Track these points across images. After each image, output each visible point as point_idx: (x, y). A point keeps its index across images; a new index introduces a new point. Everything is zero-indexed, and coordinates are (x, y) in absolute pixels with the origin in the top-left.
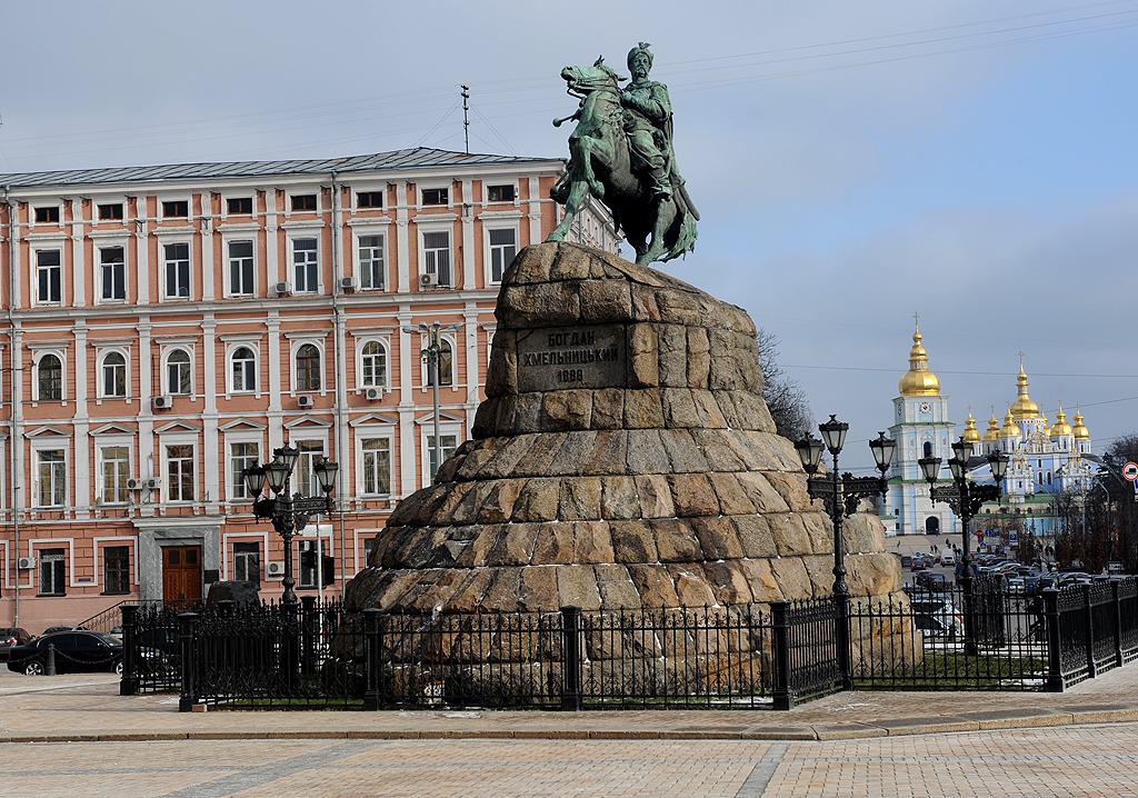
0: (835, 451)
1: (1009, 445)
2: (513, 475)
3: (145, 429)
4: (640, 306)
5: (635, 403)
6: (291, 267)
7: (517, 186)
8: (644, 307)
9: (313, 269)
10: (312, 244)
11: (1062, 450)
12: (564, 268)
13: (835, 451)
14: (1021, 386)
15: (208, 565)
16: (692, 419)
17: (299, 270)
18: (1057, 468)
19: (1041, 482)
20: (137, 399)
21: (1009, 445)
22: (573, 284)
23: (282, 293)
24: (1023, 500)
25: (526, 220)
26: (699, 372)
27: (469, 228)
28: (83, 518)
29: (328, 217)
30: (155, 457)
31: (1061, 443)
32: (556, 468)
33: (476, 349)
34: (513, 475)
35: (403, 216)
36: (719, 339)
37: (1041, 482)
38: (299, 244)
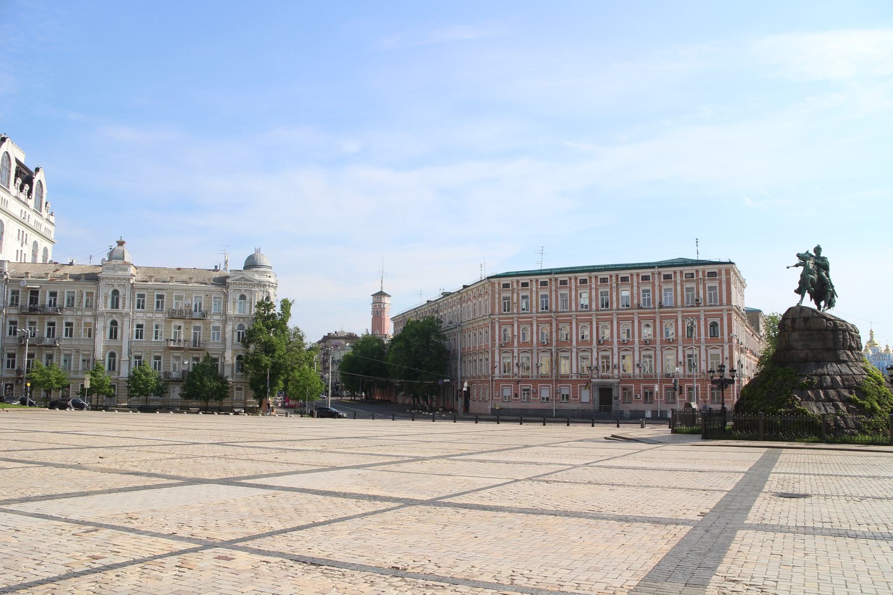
3: (595, 350)
9: (649, 299)
15: (614, 394)
17: (644, 300)
20: (591, 342)
23: (639, 307)
25: (720, 284)
27: (701, 286)
28: (575, 378)
30: (597, 359)
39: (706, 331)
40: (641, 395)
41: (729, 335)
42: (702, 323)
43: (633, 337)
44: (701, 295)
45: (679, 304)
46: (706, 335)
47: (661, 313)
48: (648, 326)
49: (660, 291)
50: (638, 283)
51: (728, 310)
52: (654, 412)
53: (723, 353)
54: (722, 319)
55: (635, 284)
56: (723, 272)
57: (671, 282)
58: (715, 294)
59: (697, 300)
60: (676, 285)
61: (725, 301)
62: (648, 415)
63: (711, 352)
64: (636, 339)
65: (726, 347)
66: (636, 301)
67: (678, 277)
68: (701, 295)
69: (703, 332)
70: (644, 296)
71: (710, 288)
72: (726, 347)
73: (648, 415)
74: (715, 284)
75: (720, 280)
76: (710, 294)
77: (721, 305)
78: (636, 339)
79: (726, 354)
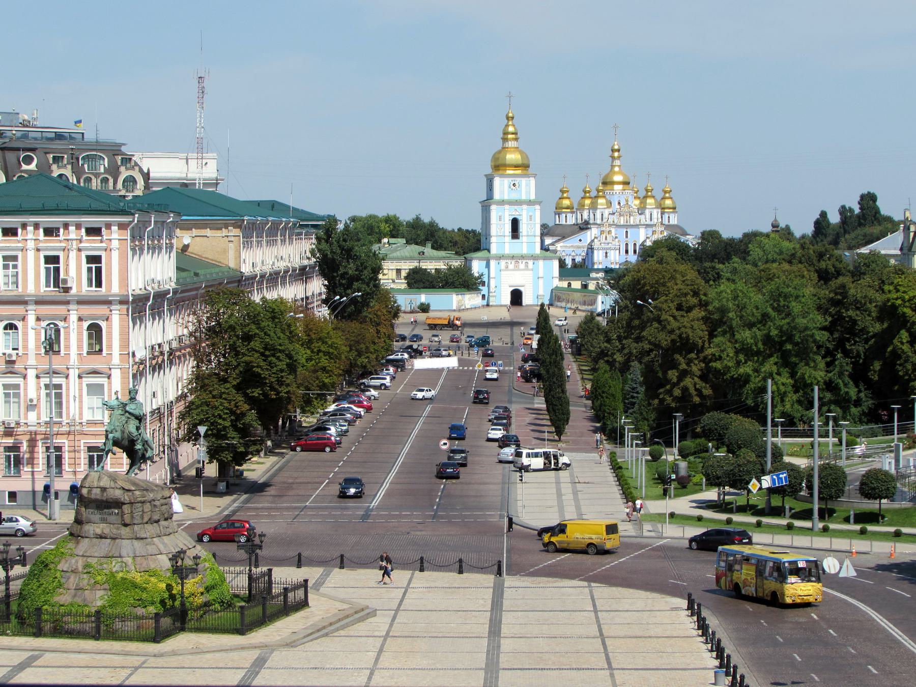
0: (182, 560)
1: (598, 216)
2: (83, 556)
4: (126, 497)
5: (125, 531)
8: (126, 498)
11: (648, 222)
12: (102, 484)
13: (182, 560)
14: (613, 158)
16: (144, 536)
19: (627, 252)
21: (598, 216)
22: (104, 489)
24: (601, 275)
26: (146, 520)
31: (648, 216)
32: (96, 555)
33: (76, 331)
34: (83, 556)
36: (155, 506)
37: (627, 252)
44: (73, 272)
46: (80, 347)
53: (110, 383)
59: (65, 281)
76: (90, 270)
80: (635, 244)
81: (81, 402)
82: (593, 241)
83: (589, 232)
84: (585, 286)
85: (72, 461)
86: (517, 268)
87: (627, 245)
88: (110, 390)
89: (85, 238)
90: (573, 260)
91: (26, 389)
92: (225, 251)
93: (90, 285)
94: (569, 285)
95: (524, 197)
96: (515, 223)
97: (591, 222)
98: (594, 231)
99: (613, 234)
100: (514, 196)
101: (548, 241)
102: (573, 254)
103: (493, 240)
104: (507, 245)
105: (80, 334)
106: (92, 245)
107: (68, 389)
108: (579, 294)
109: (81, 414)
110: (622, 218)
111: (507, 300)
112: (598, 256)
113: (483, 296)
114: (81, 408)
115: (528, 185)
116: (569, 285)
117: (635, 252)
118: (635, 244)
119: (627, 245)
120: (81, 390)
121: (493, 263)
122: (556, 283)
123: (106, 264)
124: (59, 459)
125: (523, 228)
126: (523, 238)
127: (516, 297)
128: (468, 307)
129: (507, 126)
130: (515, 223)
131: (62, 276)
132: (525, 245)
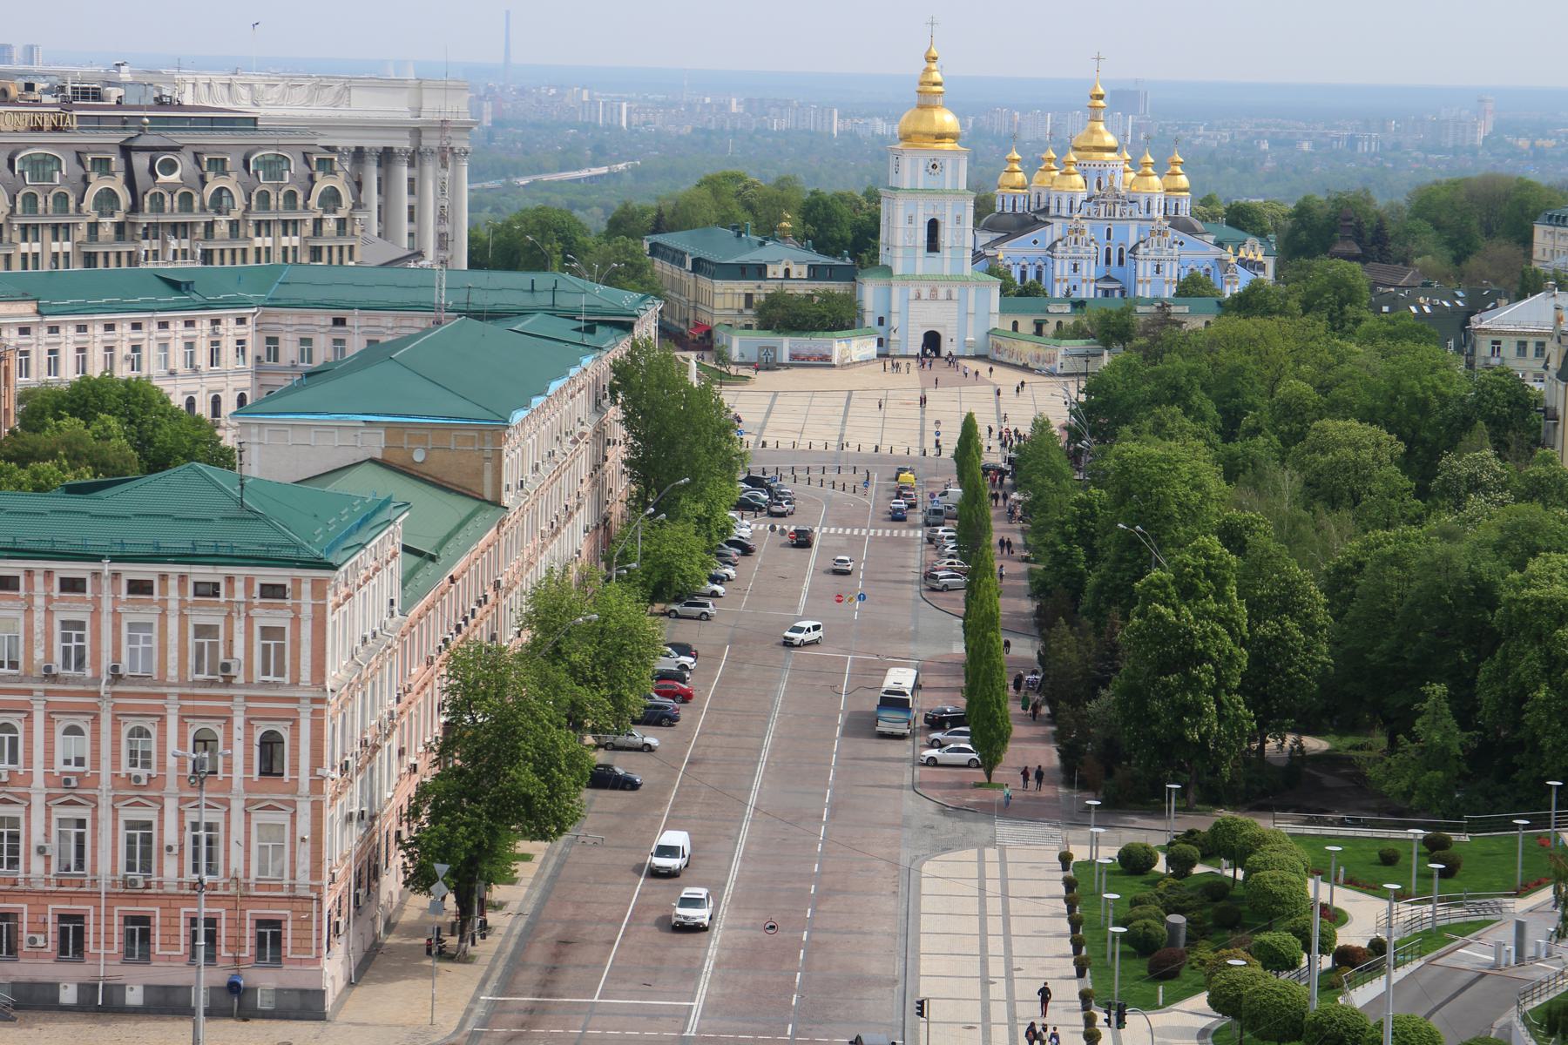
1: (1065, 204)
6: (58, 646)
7: (289, 586)
9: (80, 650)
10: (80, 625)
17: (66, 651)
18: (1132, 242)
19: (1108, 261)
21: (1065, 204)
23: (49, 675)
25: (296, 620)
27: (239, 625)
29: (97, 601)
35: (173, 605)
37: (1108, 261)
38: (65, 624)
39: (248, 757)
40: (49, 940)
41: (313, 772)
42: (238, 734)
43: (29, 761)
44: (239, 652)
45: (173, 672)
46: (248, 768)
47: (115, 694)
48: (73, 730)
49: (116, 627)
50: (49, 599)
51: (314, 700)
52: (87, 990)
54: (295, 724)
55: (39, 602)
56: (306, 587)
57: (151, 602)
58: (280, 649)
59: (226, 667)
60: (163, 615)
61: (306, 675)
62: (68, 995)
63: (259, 817)
64: (38, 770)
65: (304, 808)
66: (39, 655)
67: (173, 594)
68: (239, 652)
69: (239, 756)
70: (66, 638)
71: (267, 632)
72: (304, 808)
73: (68, 995)
74: (279, 619)
75: (296, 609)
76: (266, 648)
77: (295, 683)
78: (38, 770)
79: (304, 827)
80: (1121, 251)
81: (247, 851)
82: (1054, 245)
83: (1048, 228)
84: (1039, 328)
85: (232, 941)
86: (934, 296)
87: (1108, 250)
88: (293, 833)
89: (257, 601)
90: (1023, 274)
91: (161, 830)
92: (479, 473)
93: (266, 672)
94: (1015, 324)
95: (948, 187)
96: (933, 226)
97: (1053, 211)
98: (1056, 230)
99: (1087, 235)
100: (932, 182)
101: (985, 238)
102: (1024, 262)
103: (899, 253)
104: (919, 263)
105: (248, 746)
106: (266, 617)
107: (227, 831)
108: (1029, 345)
109: (247, 869)
110: (1102, 207)
111: (916, 348)
112: (1062, 268)
113: (880, 343)
114: (247, 861)
115: (956, 168)
116: (1015, 324)
117: (1121, 261)
118: (1121, 251)
119: (1108, 250)
120: (248, 832)
121: (896, 291)
122: (995, 322)
123: (292, 641)
124: (211, 938)
125: (946, 237)
126: (946, 253)
127: (932, 340)
128: (855, 359)
129: (928, 71)
130: (933, 226)
131: (222, 658)
132: (947, 263)
